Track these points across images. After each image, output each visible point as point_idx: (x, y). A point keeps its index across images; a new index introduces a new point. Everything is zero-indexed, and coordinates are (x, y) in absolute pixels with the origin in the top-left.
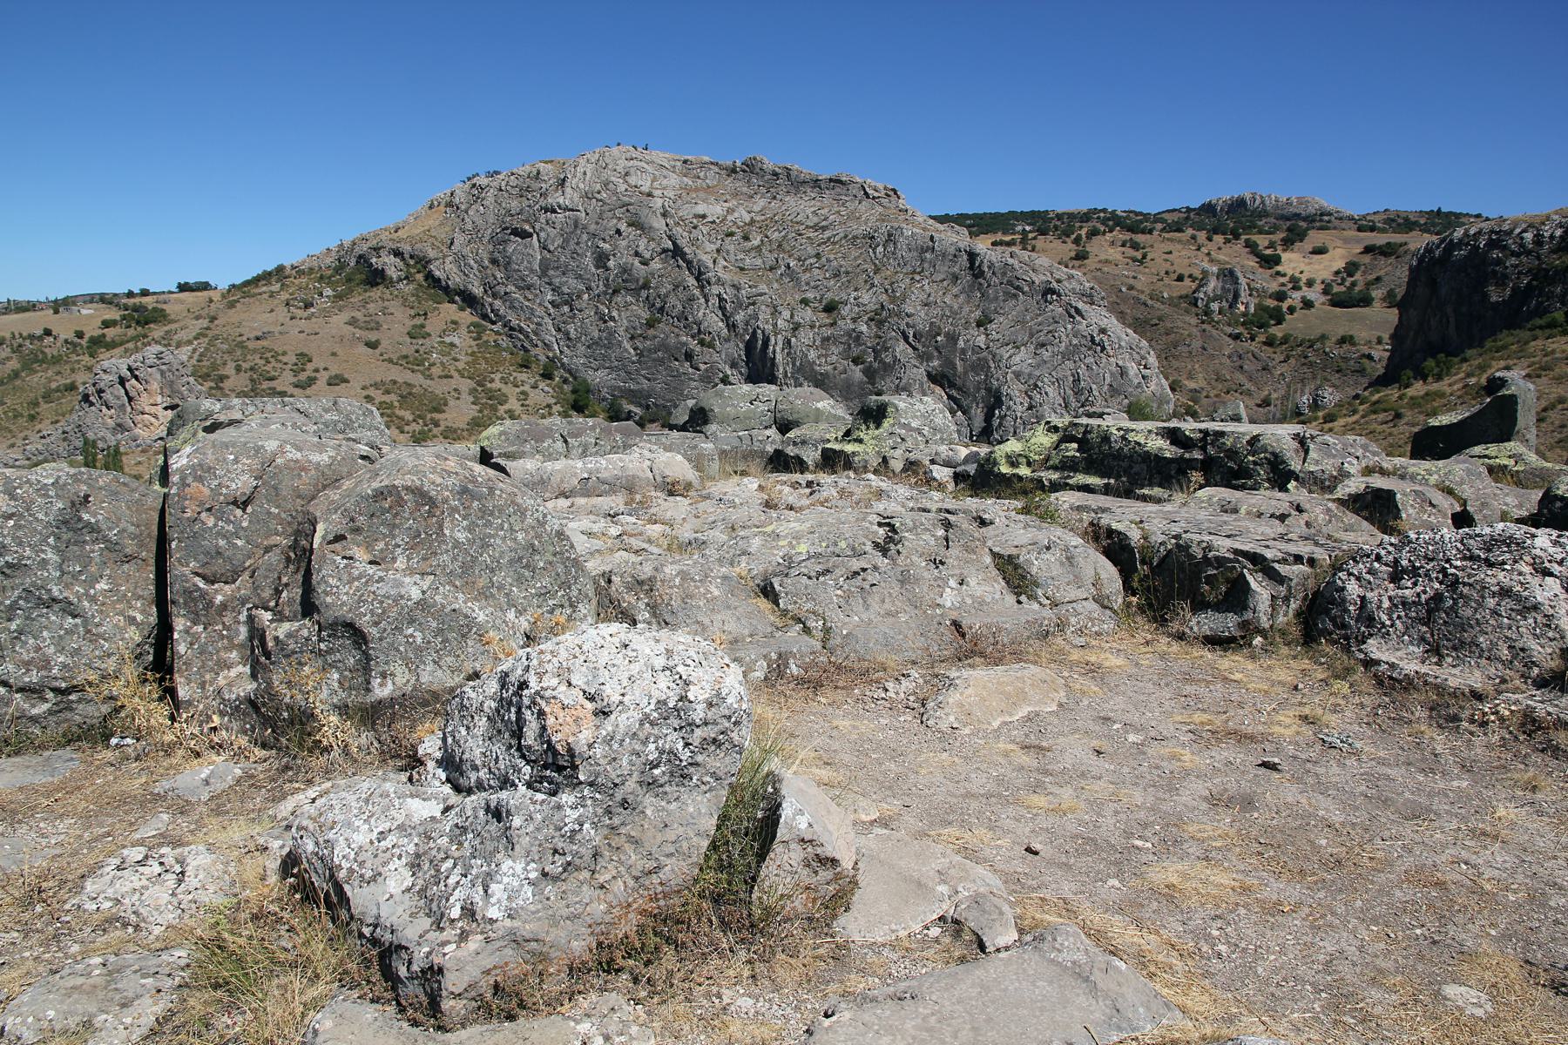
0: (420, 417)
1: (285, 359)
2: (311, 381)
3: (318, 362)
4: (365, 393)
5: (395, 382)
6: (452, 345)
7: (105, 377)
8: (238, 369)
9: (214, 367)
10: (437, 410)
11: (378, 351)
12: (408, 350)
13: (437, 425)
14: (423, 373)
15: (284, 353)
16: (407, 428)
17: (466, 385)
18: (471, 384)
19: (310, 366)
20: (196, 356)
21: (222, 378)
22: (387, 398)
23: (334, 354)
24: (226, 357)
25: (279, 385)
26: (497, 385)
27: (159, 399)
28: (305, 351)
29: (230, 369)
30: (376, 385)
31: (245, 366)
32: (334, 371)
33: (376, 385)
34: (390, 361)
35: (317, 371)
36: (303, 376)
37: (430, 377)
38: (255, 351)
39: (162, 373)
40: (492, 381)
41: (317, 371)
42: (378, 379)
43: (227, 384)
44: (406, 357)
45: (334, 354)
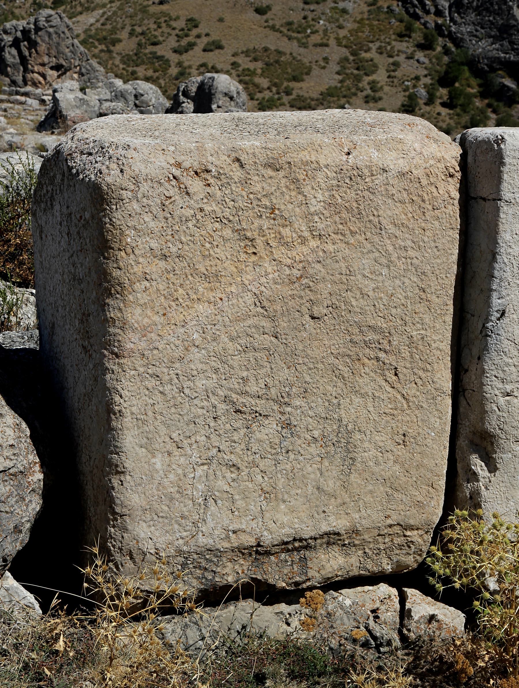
0: (275, 85)
1: (174, 24)
2: (191, 46)
3: (202, 29)
4: (234, 59)
5: (266, 49)
6: (344, 11)
7: (5, 37)
8: (132, 34)
9: (114, 31)
10: (295, 79)
11: (265, 17)
12: (296, 17)
13: (288, 93)
14: (299, 40)
15: (177, 18)
16: (259, 96)
17: (336, 53)
18: (345, 52)
19: (195, 32)
20: (102, 20)
21: (115, 42)
22: (252, 66)
23: (221, 20)
24: (128, 21)
25: (160, 50)
26: (372, 54)
27: (46, 59)
28: (196, 16)
29: (124, 35)
30: (247, 53)
31: (139, 30)
32: (214, 37)
33: (247, 53)
34: (273, 28)
35: (198, 36)
36: (184, 42)
37: (304, 45)
38: (153, 15)
39: (50, 35)
40: (368, 50)
41: (198, 36)
42: (251, 47)
43: (118, 47)
44: (290, 24)
45: (221, 20)
